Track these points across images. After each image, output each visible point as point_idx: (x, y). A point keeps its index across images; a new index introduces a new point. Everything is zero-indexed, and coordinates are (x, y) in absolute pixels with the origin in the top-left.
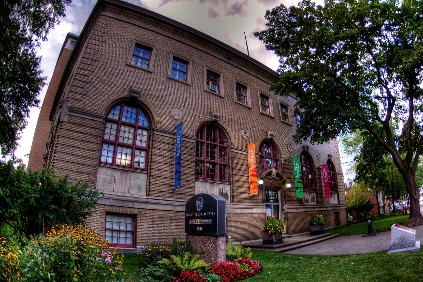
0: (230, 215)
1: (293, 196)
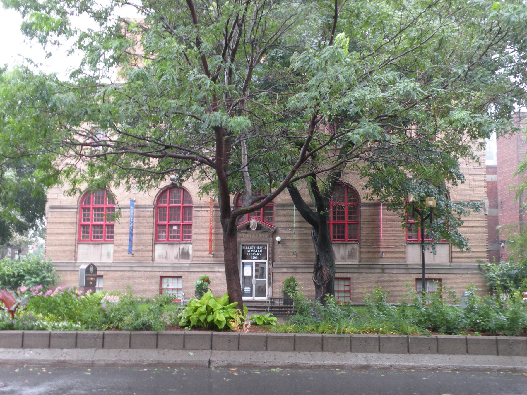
0: (186, 273)
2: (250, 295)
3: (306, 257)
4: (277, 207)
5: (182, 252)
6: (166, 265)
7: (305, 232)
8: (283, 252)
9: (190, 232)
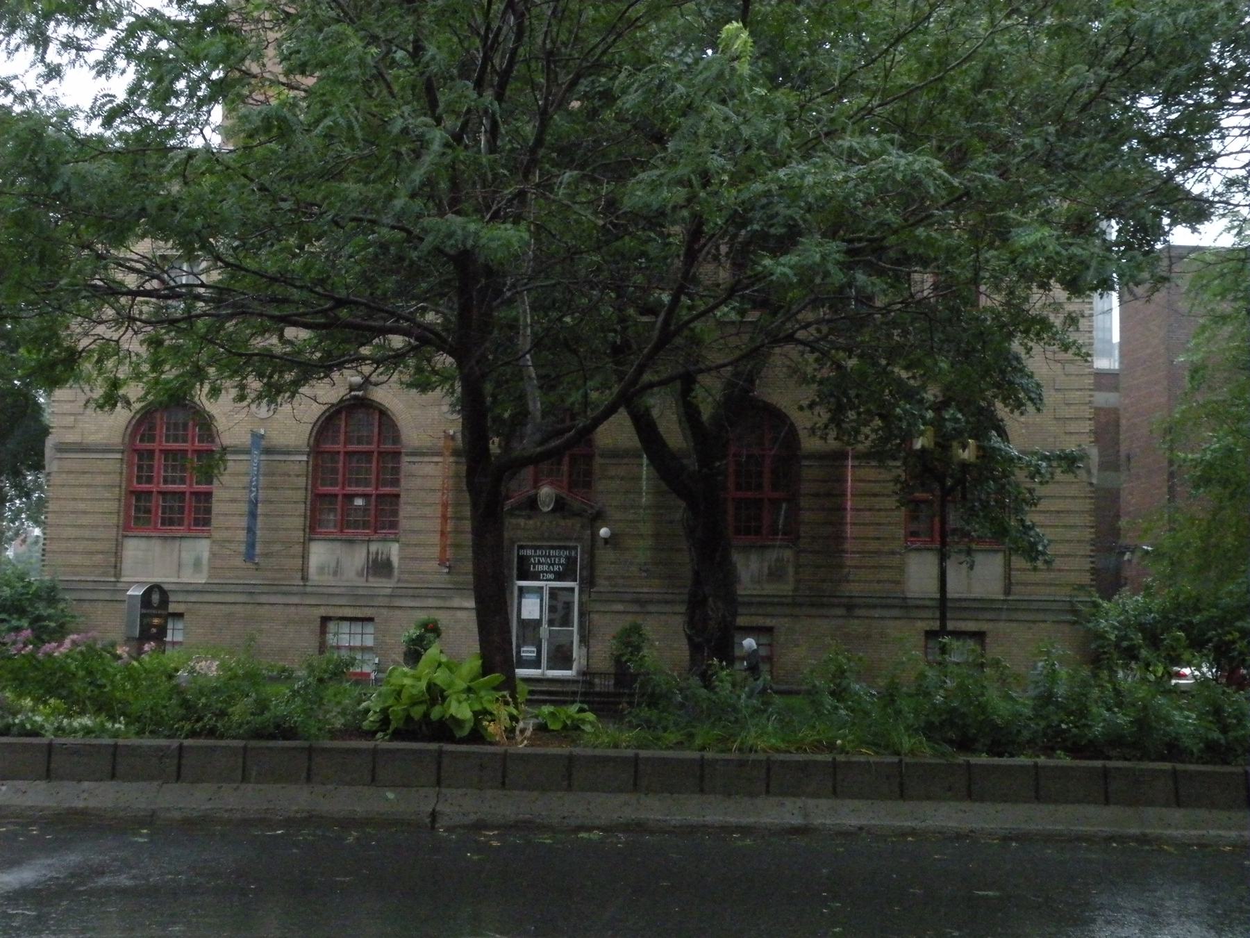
0: (384, 611)
2: (536, 664)
4: (602, 456)
5: (375, 561)
6: (336, 591)
9: (395, 513)
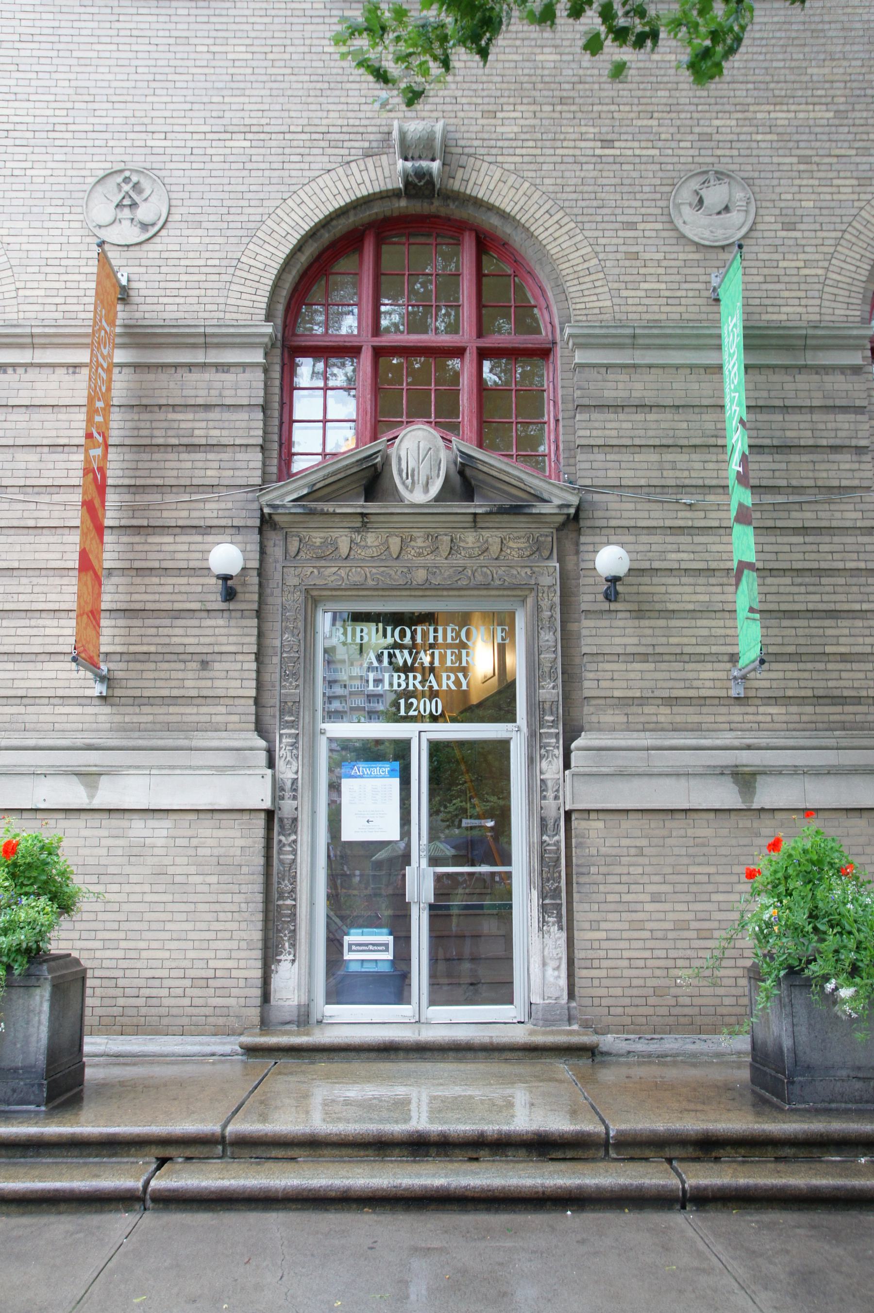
1: (702, 658)
3: (818, 699)
4: (585, 342)
7: (797, 518)
8: (644, 657)
